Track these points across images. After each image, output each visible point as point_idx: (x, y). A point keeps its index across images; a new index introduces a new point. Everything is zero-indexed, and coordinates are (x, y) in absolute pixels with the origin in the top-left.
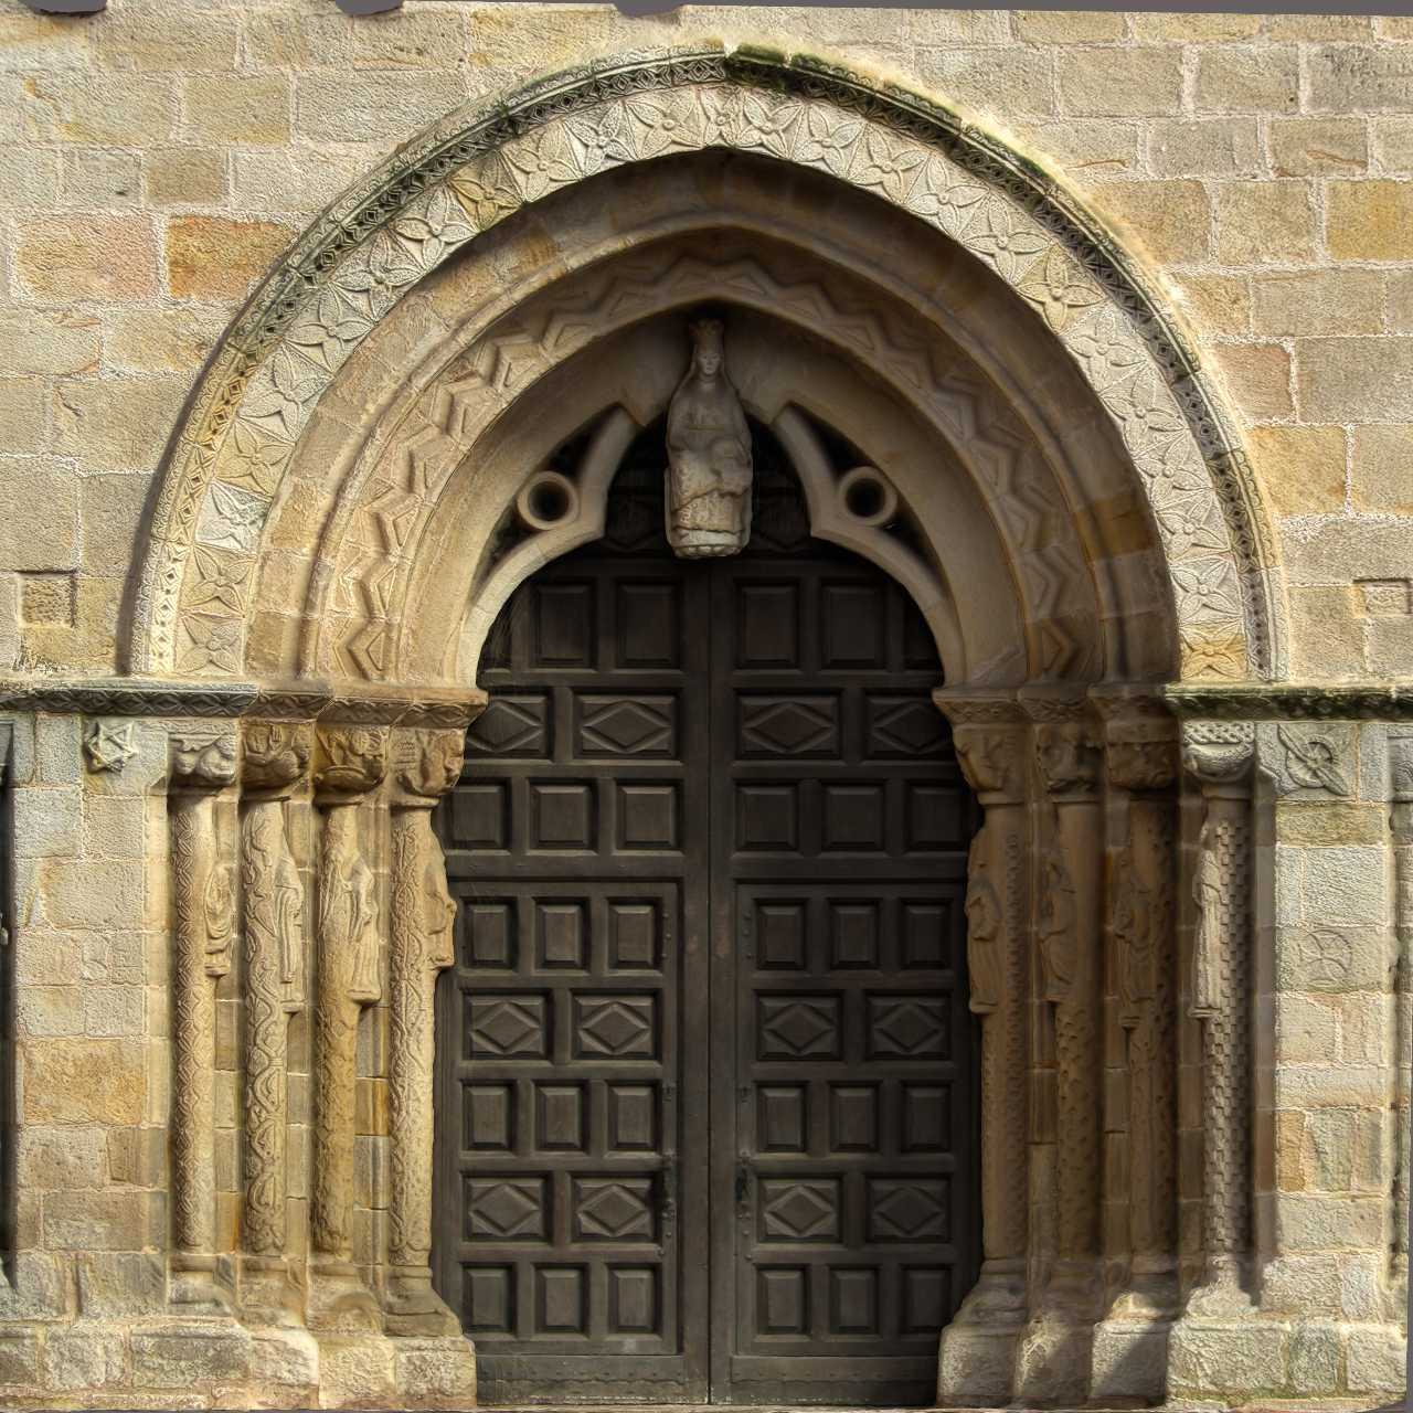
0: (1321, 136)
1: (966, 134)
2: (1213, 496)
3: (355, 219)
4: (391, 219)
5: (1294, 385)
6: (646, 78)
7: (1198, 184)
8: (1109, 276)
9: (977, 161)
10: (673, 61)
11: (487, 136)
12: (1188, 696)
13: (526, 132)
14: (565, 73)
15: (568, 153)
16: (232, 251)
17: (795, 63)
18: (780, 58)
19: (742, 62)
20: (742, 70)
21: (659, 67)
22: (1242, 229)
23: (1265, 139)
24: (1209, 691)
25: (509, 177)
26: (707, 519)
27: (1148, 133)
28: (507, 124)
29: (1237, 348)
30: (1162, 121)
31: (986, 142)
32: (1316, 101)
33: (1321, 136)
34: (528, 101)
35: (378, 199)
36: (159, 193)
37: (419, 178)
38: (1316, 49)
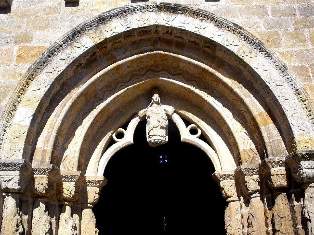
0: (304, 21)
1: (219, 18)
2: (297, 102)
3: (62, 42)
4: (72, 43)
5: (311, 75)
6: (137, 10)
7: (276, 31)
8: (260, 49)
9: (222, 25)
10: (144, 5)
11: (97, 23)
12: (303, 153)
13: (107, 23)
14: (117, 8)
15: (116, 27)
16: (31, 53)
17: (174, 5)
18: (171, 4)
19: (161, 6)
20: (161, 8)
21: (141, 7)
22: (289, 41)
23: (290, 23)
24: (309, 151)
25: (102, 32)
26: (157, 134)
27: (262, 22)
28: (102, 20)
29: (294, 67)
30: (265, 19)
31: (224, 20)
32: (300, 15)
33: (304, 21)
34: (107, 14)
35: (68, 37)
36: (16, 43)
37: (79, 33)
38: (298, 5)
